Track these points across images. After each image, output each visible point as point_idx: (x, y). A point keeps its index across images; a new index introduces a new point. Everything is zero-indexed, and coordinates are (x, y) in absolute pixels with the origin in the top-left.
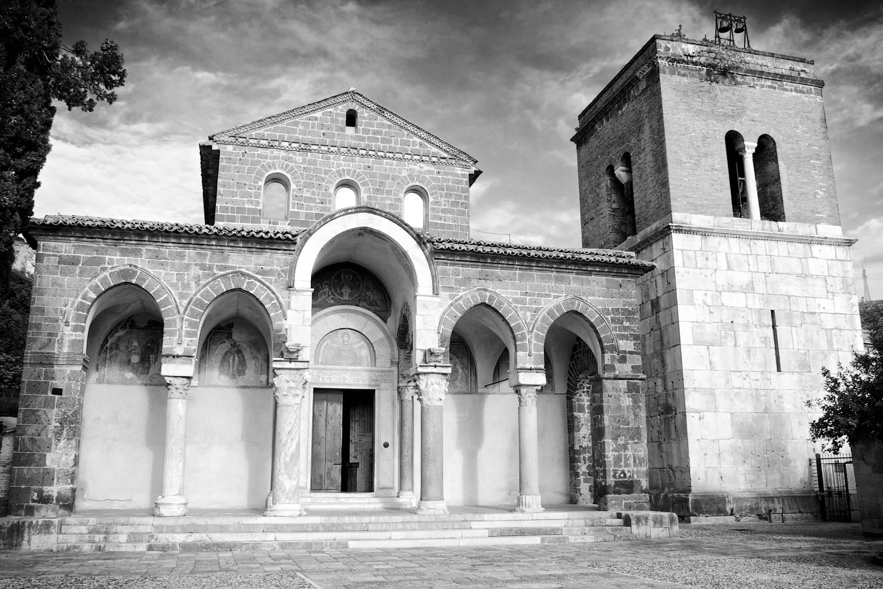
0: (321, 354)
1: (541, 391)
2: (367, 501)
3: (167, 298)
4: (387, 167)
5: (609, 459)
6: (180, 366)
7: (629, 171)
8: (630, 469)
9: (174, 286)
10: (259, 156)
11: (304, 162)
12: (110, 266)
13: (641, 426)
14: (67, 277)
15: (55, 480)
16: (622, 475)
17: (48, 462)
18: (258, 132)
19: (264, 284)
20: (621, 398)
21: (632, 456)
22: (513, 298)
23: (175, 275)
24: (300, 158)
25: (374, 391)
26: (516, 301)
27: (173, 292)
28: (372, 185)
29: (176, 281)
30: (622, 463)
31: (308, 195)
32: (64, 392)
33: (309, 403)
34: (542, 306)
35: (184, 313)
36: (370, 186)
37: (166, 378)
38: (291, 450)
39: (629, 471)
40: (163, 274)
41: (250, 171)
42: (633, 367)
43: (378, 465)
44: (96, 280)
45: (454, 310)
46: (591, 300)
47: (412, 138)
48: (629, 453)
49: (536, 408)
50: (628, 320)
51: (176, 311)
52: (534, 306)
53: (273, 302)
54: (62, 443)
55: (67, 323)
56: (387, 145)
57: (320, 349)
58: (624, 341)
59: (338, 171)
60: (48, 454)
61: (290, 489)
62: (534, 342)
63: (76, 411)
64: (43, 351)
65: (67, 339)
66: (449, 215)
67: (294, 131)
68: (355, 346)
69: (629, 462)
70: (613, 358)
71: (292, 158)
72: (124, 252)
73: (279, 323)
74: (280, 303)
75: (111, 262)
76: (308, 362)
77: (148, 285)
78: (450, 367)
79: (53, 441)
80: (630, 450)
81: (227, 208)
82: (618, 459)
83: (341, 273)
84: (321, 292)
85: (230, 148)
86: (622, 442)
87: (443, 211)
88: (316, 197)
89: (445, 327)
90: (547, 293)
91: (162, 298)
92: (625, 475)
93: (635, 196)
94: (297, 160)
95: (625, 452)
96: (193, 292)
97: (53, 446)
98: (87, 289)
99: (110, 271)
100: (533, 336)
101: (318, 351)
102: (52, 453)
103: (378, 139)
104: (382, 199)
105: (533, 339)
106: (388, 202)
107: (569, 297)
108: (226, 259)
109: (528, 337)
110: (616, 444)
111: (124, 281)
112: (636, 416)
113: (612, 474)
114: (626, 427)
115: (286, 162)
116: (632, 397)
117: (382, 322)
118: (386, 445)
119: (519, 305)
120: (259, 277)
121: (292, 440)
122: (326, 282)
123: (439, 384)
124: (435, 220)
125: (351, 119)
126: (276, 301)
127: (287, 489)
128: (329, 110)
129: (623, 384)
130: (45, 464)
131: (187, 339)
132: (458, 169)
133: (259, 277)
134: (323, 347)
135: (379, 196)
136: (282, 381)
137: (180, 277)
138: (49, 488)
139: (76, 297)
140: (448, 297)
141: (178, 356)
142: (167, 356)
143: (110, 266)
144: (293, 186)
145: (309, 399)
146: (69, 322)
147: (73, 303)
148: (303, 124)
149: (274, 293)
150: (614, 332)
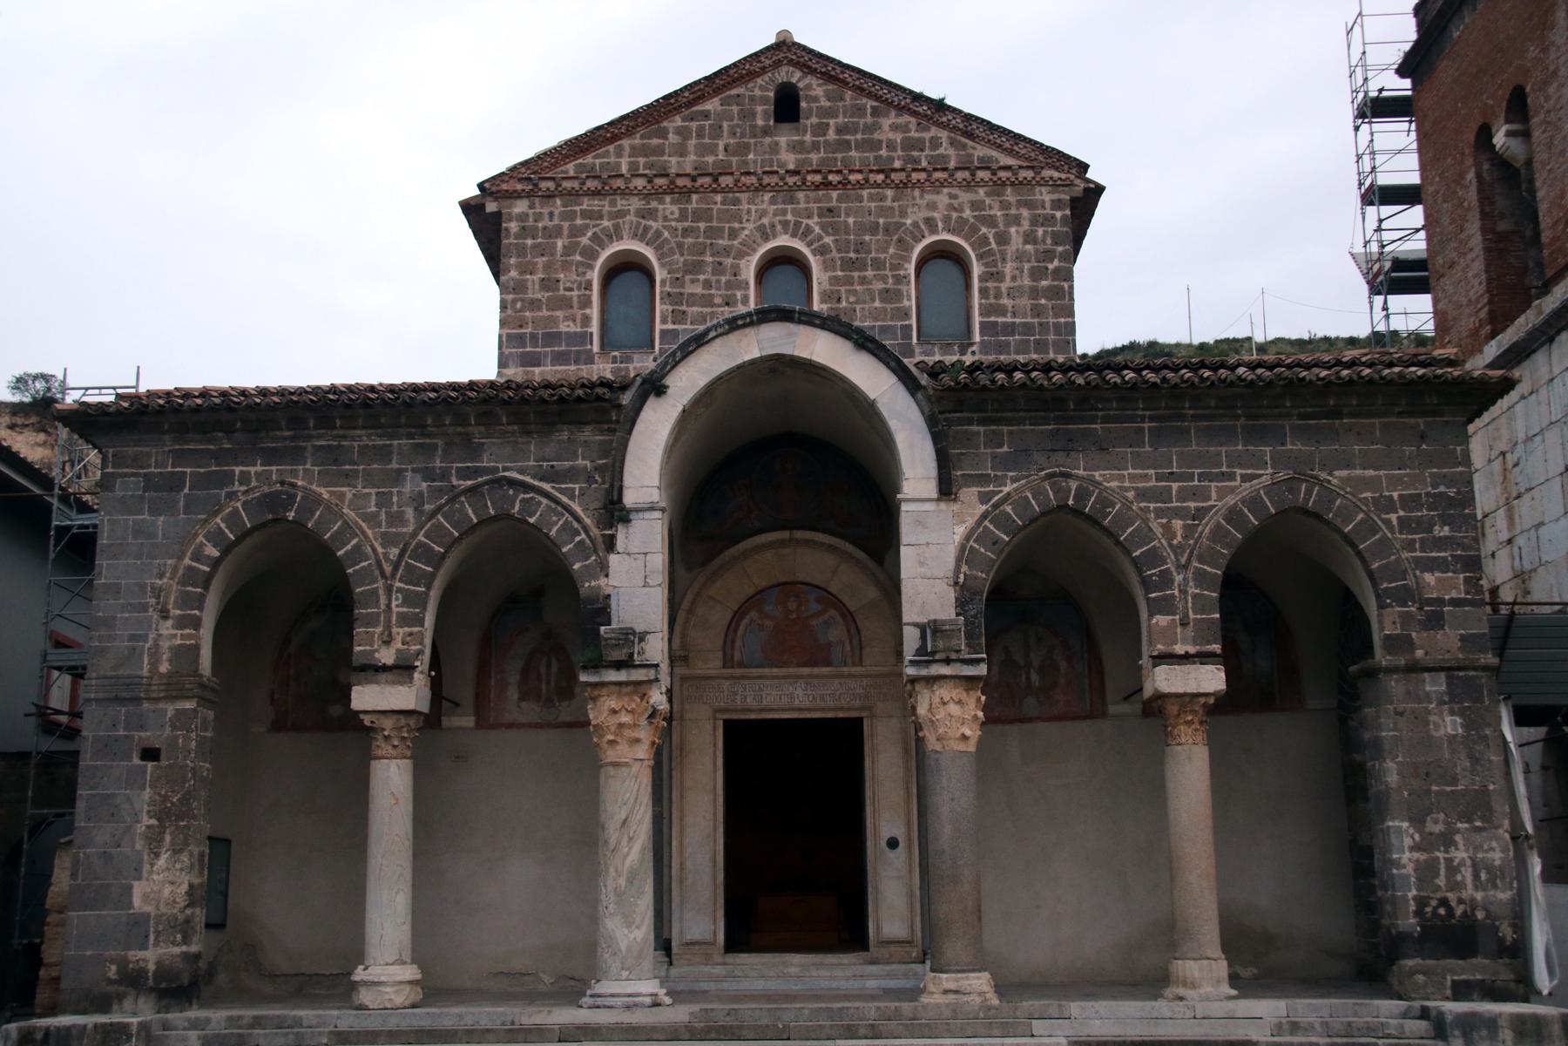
0: (738, 643)
2: (849, 973)
3: (357, 547)
4: (873, 205)
5: (1404, 871)
6: (388, 689)
8: (1464, 895)
9: (372, 519)
10: (587, 214)
11: (683, 216)
12: (243, 488)
13: (1491, 787)
14: (162, 518)
15: (152, 937)
16: (1442, 911)
17: (137, 901)
18: (581, 161)
20: (1433, 718)
21: (1469, 862)
22: (1136, 489)
23: (374, 497)
24: (675, 208)
25: (860, 720)
26: (1142, 495)
27: (369, 533)
28: (839, 251)
29: (374, 509)
30: (1441, 881)
32: (163, 755)
33: (715, 752)
34: (1211, 503)
35: (393, 576)
36: (834, 254)
37: (362, 716)
38: (629, 859)
39: (1461, 901)
40: (349, 496)
41: (569, 250)
42: (1463, 638)
43: (876, 888)
44: (218, 520)
45: (992, 527)
46: (1340, 478)
48: (1460, 854)
49: (1206, 748)
50: (1445, 521)
51: (377, 573)
52: (1192, 505)
53: (578, 539)
54: (162, 862)
55: (165, 615)
56: (871, 155)
57: (735, 631)
58: (1437, 574)
60: (136, 884)
61: (629, 949)
62: (1193, 590)
63: (188, 792)
64: (120, 672)
65: (165, 644)
68: (814, 622)
69: (1459, 878)
70: (1406, 619)
71: (656, 210)
72: (271, 457)
73: (593, 584)
75: (245, 478)
76: (657, 666)
77: (317, 523)
78: (982, 660)
79: (146, 857)
80: (1461, 846)
81: (521, 337)
82: (1426, 871)
85: (520, 207)
86: (1438, 828)
88: (713, 292)
89: (970, 568)
90: (1224, 469)
91: (349, 547)
92: (1450, 910)
93: (1540, 195)
94: (668, 213)
95: (1446, 852)
96: (411, 528)
97: (146, 867)
98: (201, 538)
99: (243, 498)
100: (1190, 576)
101: (730, 637)
102: (144, 883)
103: (848, 142)
105: (1191, 584)
107: (1281, 476)
108: (475, 452)
109: (1178, 578)
110: (1421, 832)
111: (270, 516)
112: (1475, 760)
113: (1412, 907)
114: (1449, 789)
115: (643, 222)
116: (1461, 713)
117: (871, 564)
118: (893, 843)
119: (1152, 506)
120: (546, 486)
121: (630, 839)
123: (959, 702)
124: (989, 317)
125: (787, 107)
126: (583, 536)
127: (623, 949)
128: (734, 92)
129: (1435, 685)
130: (130, 905)
131: (401, 631)
132: (1044, 190)
133: (546, 486)
134: (742, 627)
135: (856, 274)
136: (604, 711)
137: (383, 500)
138: (140, 954)
139: (181, 558)
140: (975, 498)
141: (385, 668)
143: (243, 488)
144: (660, 274)
145: (715, 745)
146: (168, 611)
147: (175, 569)
150: (1406, 555)
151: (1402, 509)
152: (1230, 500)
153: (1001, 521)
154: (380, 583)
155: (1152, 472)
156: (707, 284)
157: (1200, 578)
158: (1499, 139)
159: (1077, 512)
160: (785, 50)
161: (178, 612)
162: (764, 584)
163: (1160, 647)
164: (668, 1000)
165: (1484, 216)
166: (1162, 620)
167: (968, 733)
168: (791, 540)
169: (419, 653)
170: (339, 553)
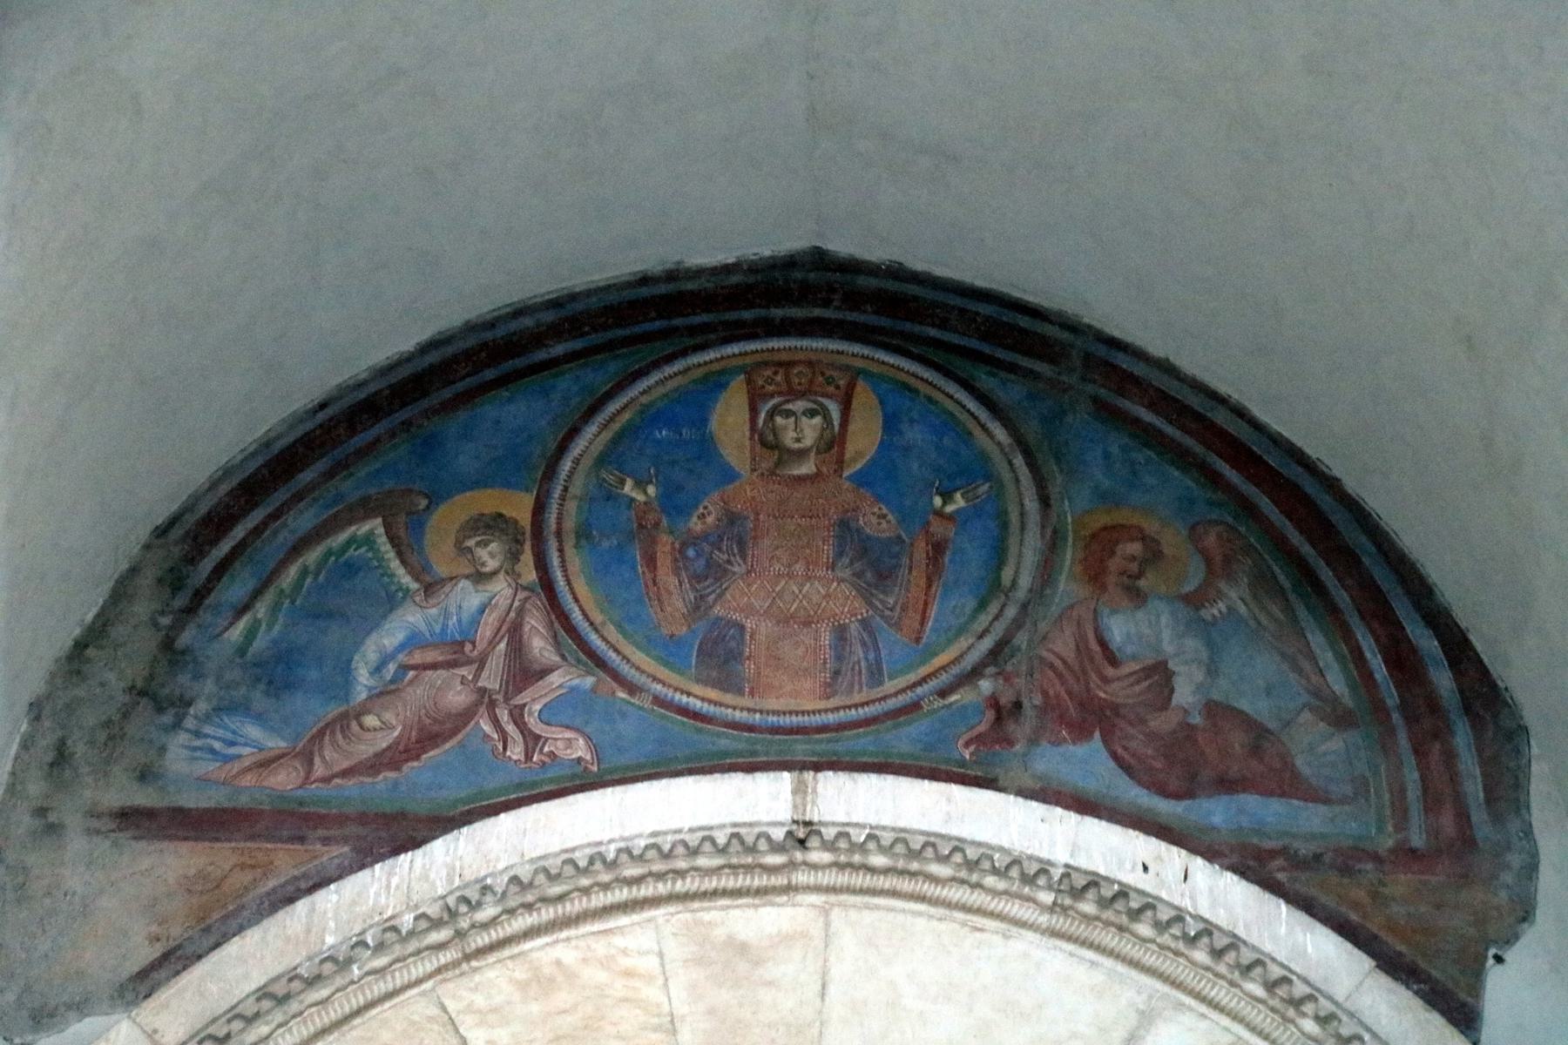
83: (714, 382)
84: (390, 635)
122: (488, 501)
168: (803, 835)
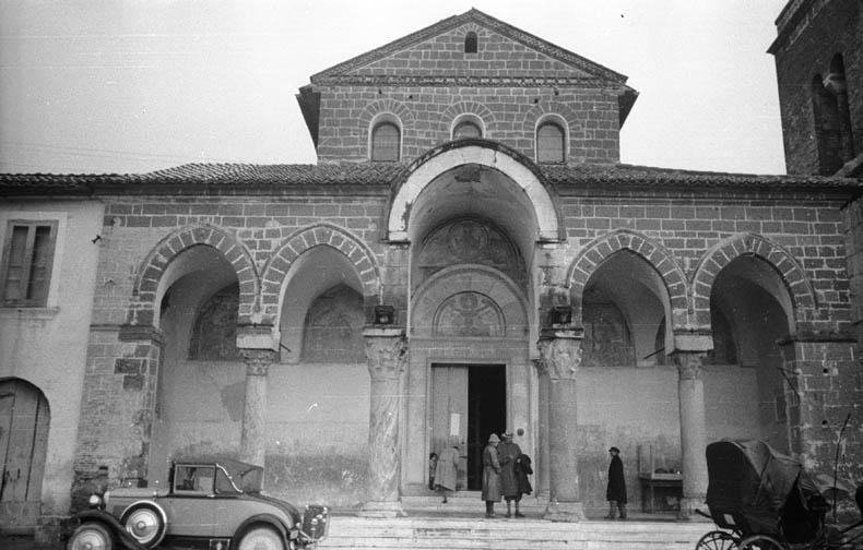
1: (711, 358)
3: (243, 259)
7: (841, 78)
19: (352, 238)
26: (670, 244)
31: (423, 137)
35: (262, 276)
36: (495, 121)
47: (544, 58)
52: (695, 250)
59: (456, 107)
62: (695, 294)
66: (593, 148)
67: (405, 63)
72: (197, 210)
74: (372, 259)
87: (587, 144)
104: (509, 135)
106: (517, 138)
109: (687, 289)
115: (396, 101)
125: (471, 45)
131: (266, 306)
142: (243, 326)
148: (415, 54)
149: (364, 247)
151: (807, 255)
152: (717, 247)
153: (593, 256)
154: (254, 280)
155: (673, 231)
156: (428, 135)
157: (700, 289)
158: (827, 81)
159: (633, 252)
160: (474, 16)
161: (143, 293)
162: (454, 292)
163: (679, 326)
164: (405, 514)
165: (817, 121)
166: (678, 311)
167: (573, 369)
169: (274, 318)
170: (233, 263)
